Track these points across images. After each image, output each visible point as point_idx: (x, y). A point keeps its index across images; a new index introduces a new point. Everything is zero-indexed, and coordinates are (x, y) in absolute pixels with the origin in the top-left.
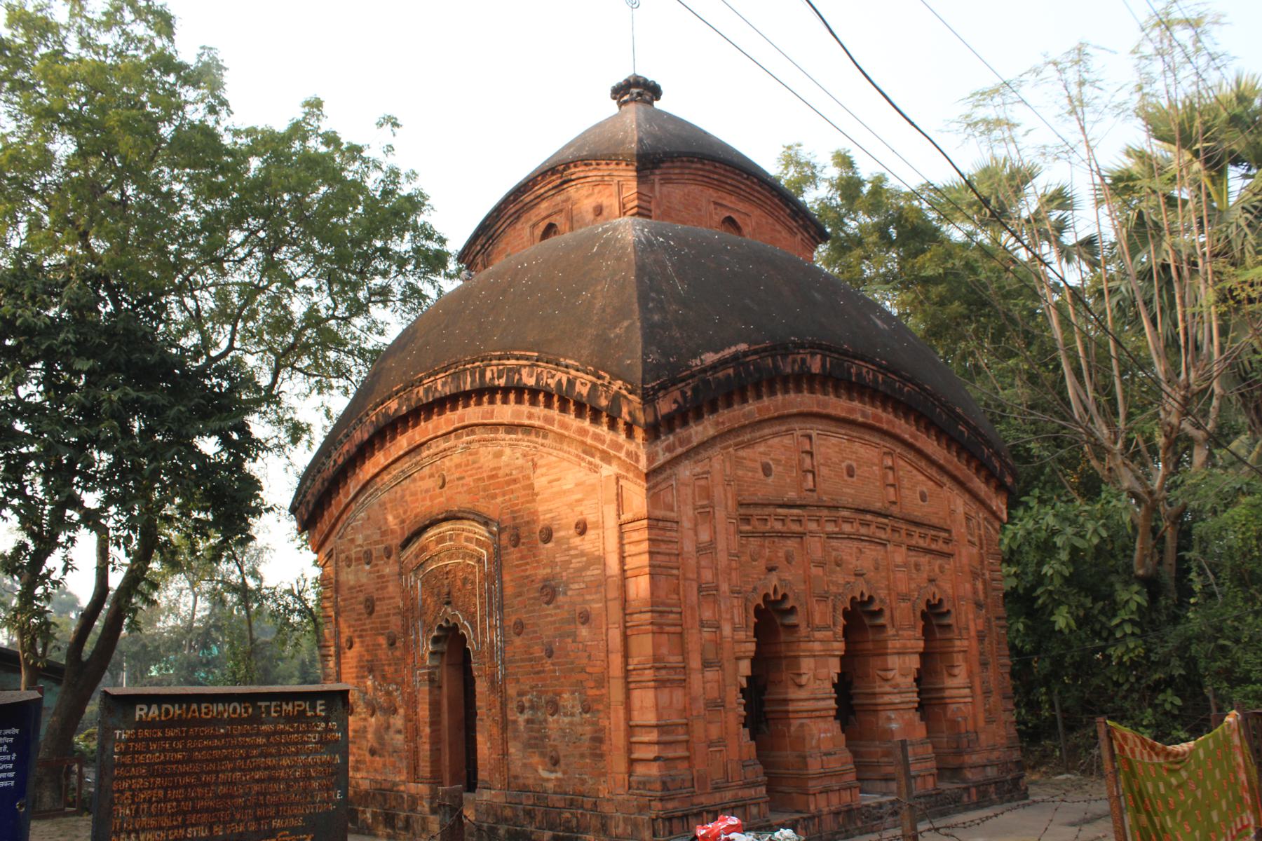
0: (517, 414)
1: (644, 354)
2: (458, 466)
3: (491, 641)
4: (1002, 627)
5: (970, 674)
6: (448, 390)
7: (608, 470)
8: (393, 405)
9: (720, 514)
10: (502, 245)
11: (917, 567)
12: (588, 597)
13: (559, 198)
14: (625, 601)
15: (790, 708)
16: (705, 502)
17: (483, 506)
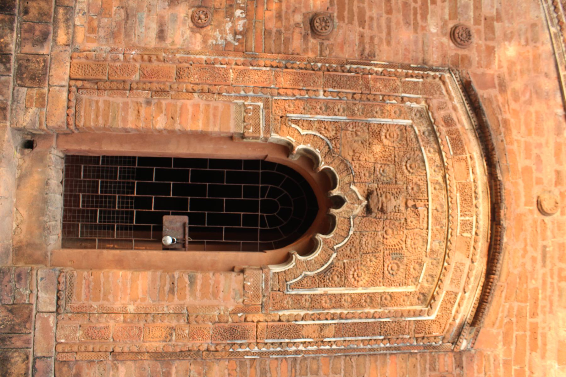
3: (296, 332)
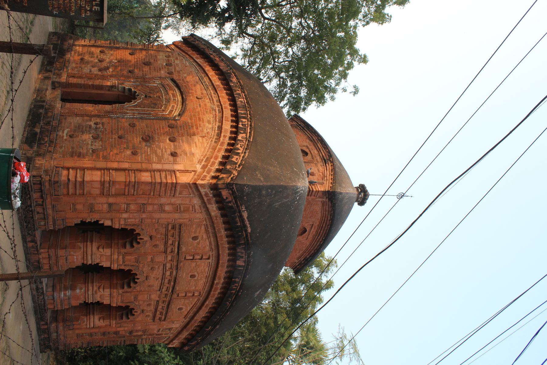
0: (226, 131)
1: (248, 185)
2: (205, 105)
3: (128, 113)
4: (121, 343)
5: (100, 327)
6: (238, 103)
7: (199, 168)
8: (234, 80)
9: (177, 216)
10: (300, 133)
11: (149, 305)
12: (144, 155)
13: (318, 158)
14: (141, 171)
15: (89, 243)
16: (182, 209)
17: (187, 114)
